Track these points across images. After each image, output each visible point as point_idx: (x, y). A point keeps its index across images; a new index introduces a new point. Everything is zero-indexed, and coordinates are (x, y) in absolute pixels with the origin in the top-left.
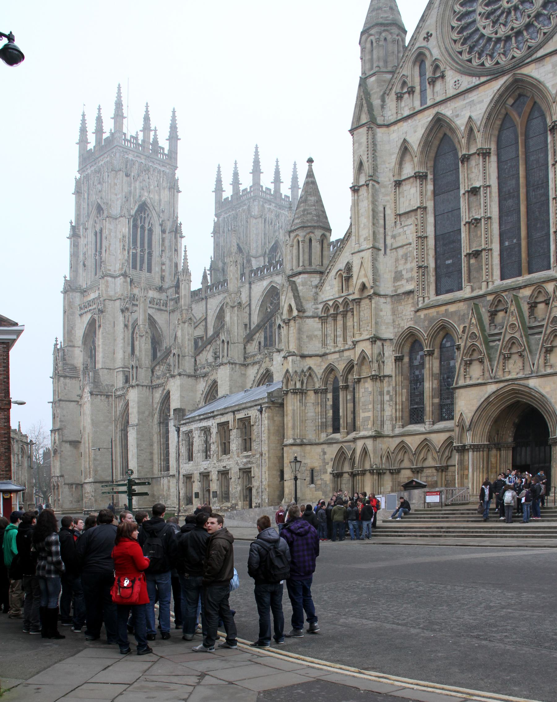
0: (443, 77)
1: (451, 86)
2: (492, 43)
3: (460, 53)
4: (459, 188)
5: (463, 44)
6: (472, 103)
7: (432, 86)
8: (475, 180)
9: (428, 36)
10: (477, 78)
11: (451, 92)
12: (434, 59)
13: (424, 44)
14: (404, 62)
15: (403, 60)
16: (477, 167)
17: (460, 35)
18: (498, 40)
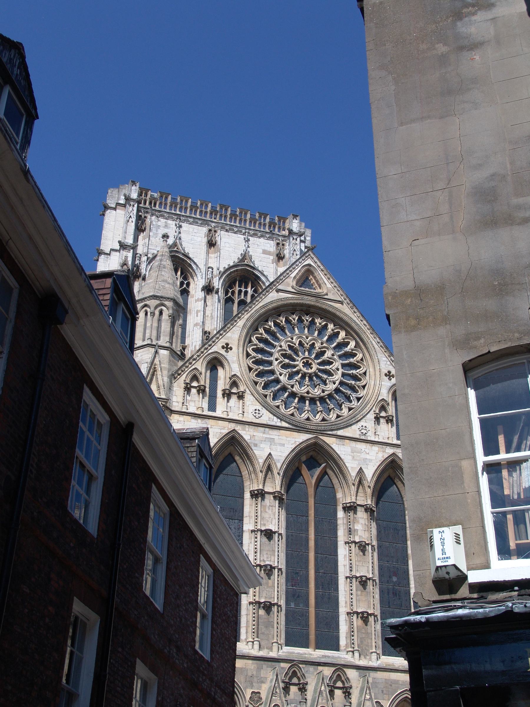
0: (241, 397)
1: (250, 412)
2: (287, 393)
3: (256, 383)
4: (241, 520)
5: (257, 375)
6: (272, 441)
7: (226, 398)
8: (268, 521)
9: (227, 347)
10: (279, 420)
11: (249, 417)
12: (233, 374)
13: (223, 352)
14: (198, 356)
15: (198, 354)
16: (271, 508)
17: (257, 367)
18: (293, 395)
